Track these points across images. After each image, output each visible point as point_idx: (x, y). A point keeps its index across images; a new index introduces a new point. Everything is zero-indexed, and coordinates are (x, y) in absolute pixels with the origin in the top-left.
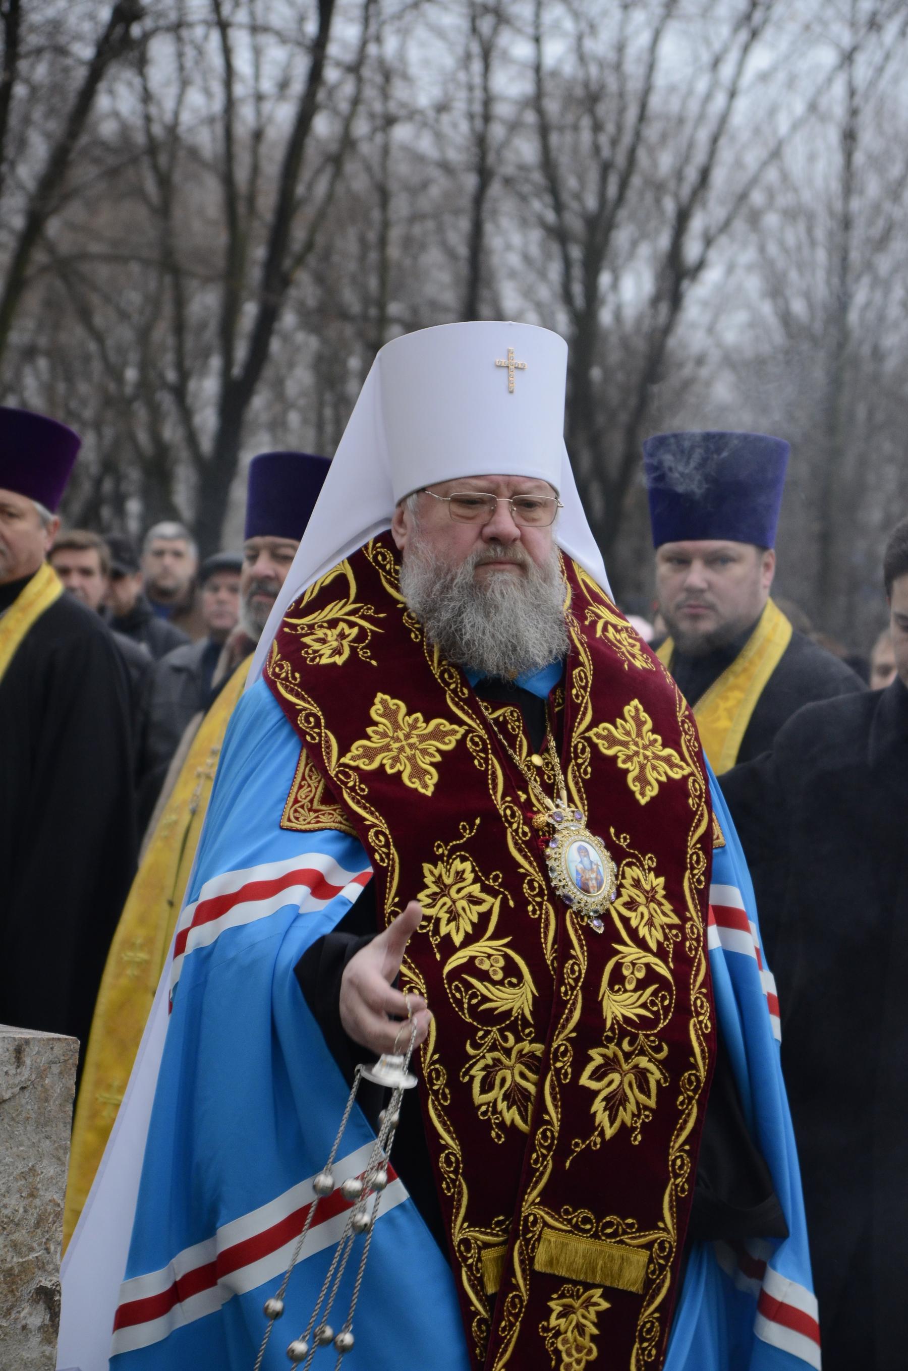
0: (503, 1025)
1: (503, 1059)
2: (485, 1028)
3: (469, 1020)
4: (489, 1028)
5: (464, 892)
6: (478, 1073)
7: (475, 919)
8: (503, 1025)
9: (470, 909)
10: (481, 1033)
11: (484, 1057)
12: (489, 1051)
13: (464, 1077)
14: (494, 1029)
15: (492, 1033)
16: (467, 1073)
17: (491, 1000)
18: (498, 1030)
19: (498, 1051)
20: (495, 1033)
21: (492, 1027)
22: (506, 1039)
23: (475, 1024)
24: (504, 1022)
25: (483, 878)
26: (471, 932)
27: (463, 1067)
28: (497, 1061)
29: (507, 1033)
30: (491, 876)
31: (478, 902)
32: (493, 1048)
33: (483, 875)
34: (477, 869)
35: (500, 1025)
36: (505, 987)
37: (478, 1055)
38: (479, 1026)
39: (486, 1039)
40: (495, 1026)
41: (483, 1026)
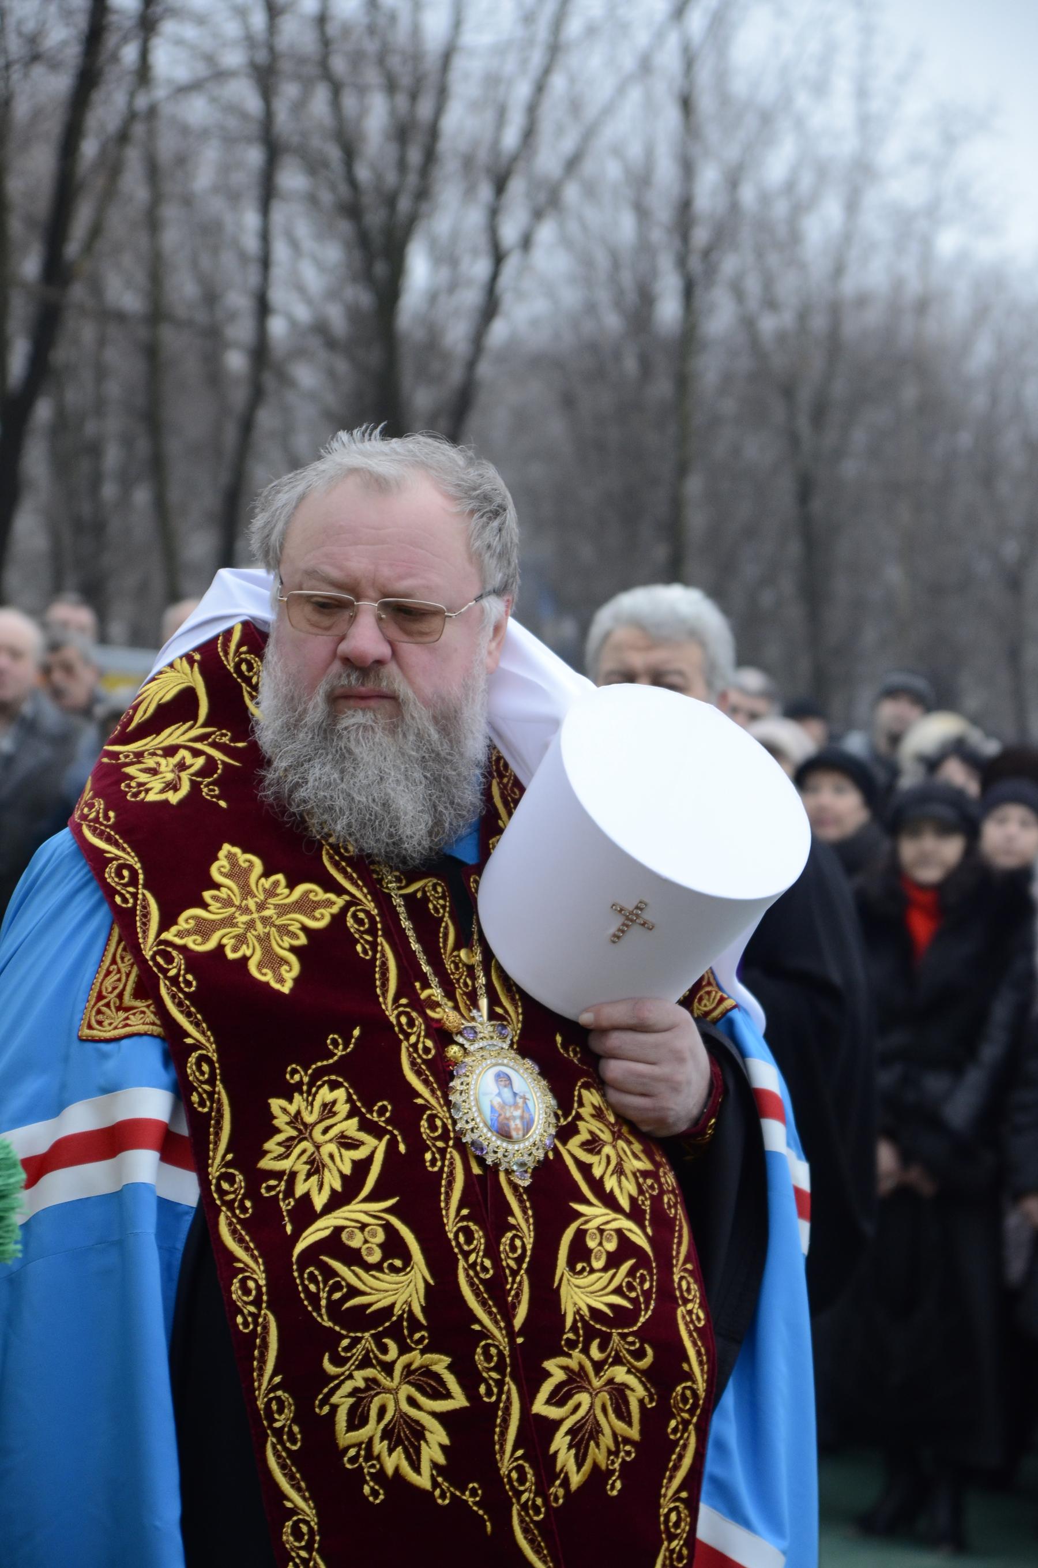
1: (381, 1377)
2: (352, 1334)
3: (328, 1324)
4: (359, 1335)
6: (343, 1401)
10: (345, 1342)
11: (350, 1377)
12: (359, 1367)
13: (321, 1407)
14: (367, 1335)
15: (363, 1342)
16: (325, 1401)
18: (372, 1336)
19: (373, 1366)
21: (364, 1331)
22: (384, 1349)
23: (337, 1328)
27: (320, 1392)
28: (372, 1383)
29: (386, 1340)
32: (365, 1363)
35: (375, 1329)
37: (343, 1374)
38: (344, 1332)
39: (354, 1351)
40: (367, 1330)
41: (349, 1331)
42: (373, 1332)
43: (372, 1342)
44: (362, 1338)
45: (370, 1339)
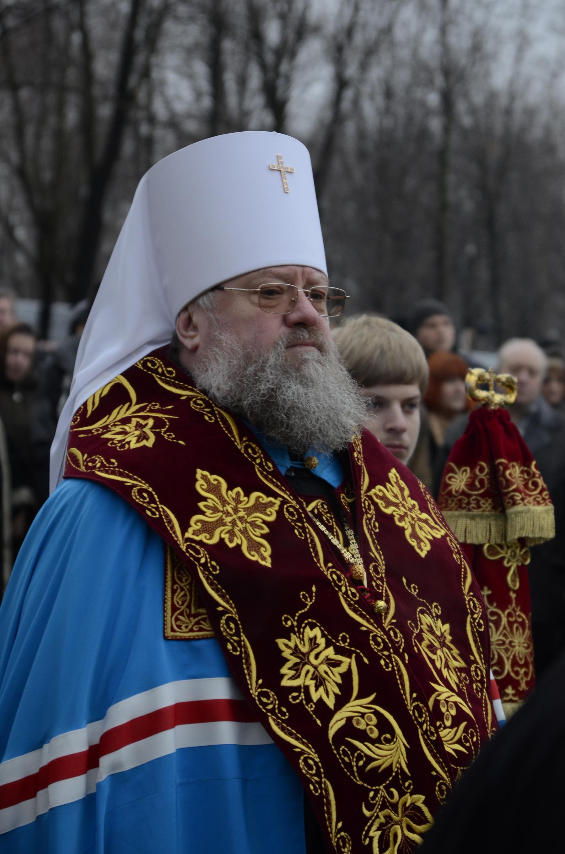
0: (388, 782)
2: (374, 788)
4: (377, 787)
5: (322, 657)
7: (339, 681)
8: (388, 782)
9: (332, 672)
10: (371, 794)
12: (381, 810)
14: (381, 787)
15: (381, 792)
17: (375, 760)
20: (382, 791)
21: (379, 786)
24: (388, 779)
25: (334, 641)
26: (340, 693)
30: (340, 638)
31: (337, 664)
32: (383, 807)
33: (333, 638)
34: (326, 632)
36: (382, 744)
39: (377, 799)
40: (381, 784)
41: (372, 786)
42: (384, 784)
43: (385, 791)
44: (379, 790)
45: (384, 790)
